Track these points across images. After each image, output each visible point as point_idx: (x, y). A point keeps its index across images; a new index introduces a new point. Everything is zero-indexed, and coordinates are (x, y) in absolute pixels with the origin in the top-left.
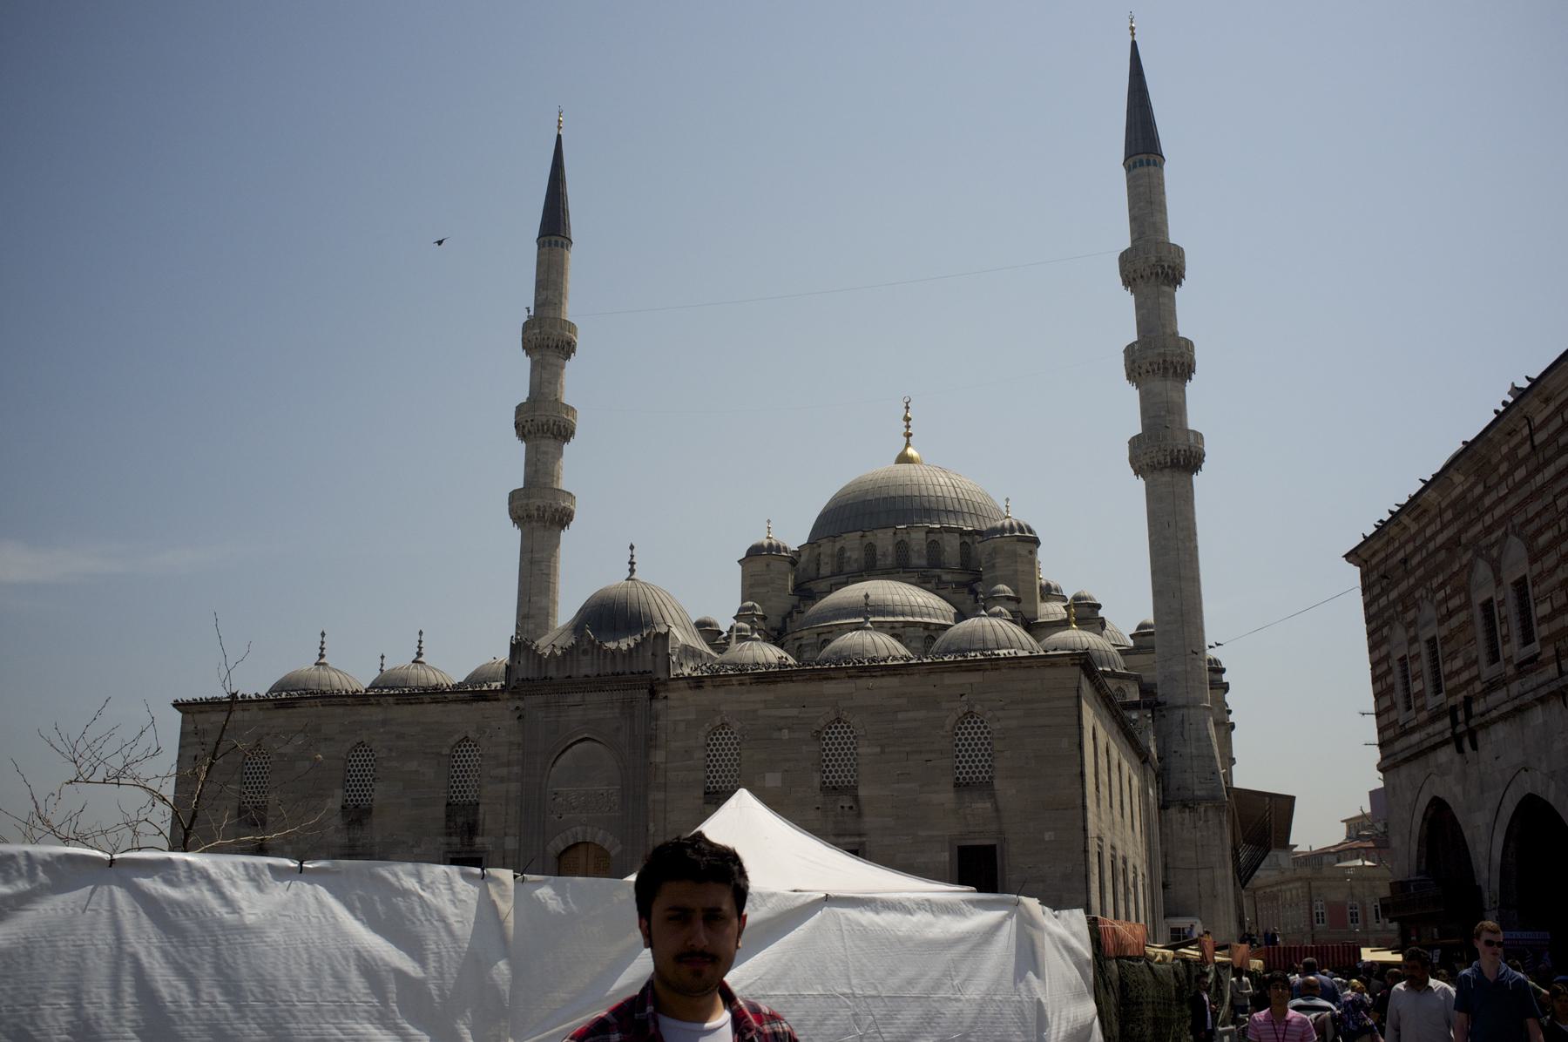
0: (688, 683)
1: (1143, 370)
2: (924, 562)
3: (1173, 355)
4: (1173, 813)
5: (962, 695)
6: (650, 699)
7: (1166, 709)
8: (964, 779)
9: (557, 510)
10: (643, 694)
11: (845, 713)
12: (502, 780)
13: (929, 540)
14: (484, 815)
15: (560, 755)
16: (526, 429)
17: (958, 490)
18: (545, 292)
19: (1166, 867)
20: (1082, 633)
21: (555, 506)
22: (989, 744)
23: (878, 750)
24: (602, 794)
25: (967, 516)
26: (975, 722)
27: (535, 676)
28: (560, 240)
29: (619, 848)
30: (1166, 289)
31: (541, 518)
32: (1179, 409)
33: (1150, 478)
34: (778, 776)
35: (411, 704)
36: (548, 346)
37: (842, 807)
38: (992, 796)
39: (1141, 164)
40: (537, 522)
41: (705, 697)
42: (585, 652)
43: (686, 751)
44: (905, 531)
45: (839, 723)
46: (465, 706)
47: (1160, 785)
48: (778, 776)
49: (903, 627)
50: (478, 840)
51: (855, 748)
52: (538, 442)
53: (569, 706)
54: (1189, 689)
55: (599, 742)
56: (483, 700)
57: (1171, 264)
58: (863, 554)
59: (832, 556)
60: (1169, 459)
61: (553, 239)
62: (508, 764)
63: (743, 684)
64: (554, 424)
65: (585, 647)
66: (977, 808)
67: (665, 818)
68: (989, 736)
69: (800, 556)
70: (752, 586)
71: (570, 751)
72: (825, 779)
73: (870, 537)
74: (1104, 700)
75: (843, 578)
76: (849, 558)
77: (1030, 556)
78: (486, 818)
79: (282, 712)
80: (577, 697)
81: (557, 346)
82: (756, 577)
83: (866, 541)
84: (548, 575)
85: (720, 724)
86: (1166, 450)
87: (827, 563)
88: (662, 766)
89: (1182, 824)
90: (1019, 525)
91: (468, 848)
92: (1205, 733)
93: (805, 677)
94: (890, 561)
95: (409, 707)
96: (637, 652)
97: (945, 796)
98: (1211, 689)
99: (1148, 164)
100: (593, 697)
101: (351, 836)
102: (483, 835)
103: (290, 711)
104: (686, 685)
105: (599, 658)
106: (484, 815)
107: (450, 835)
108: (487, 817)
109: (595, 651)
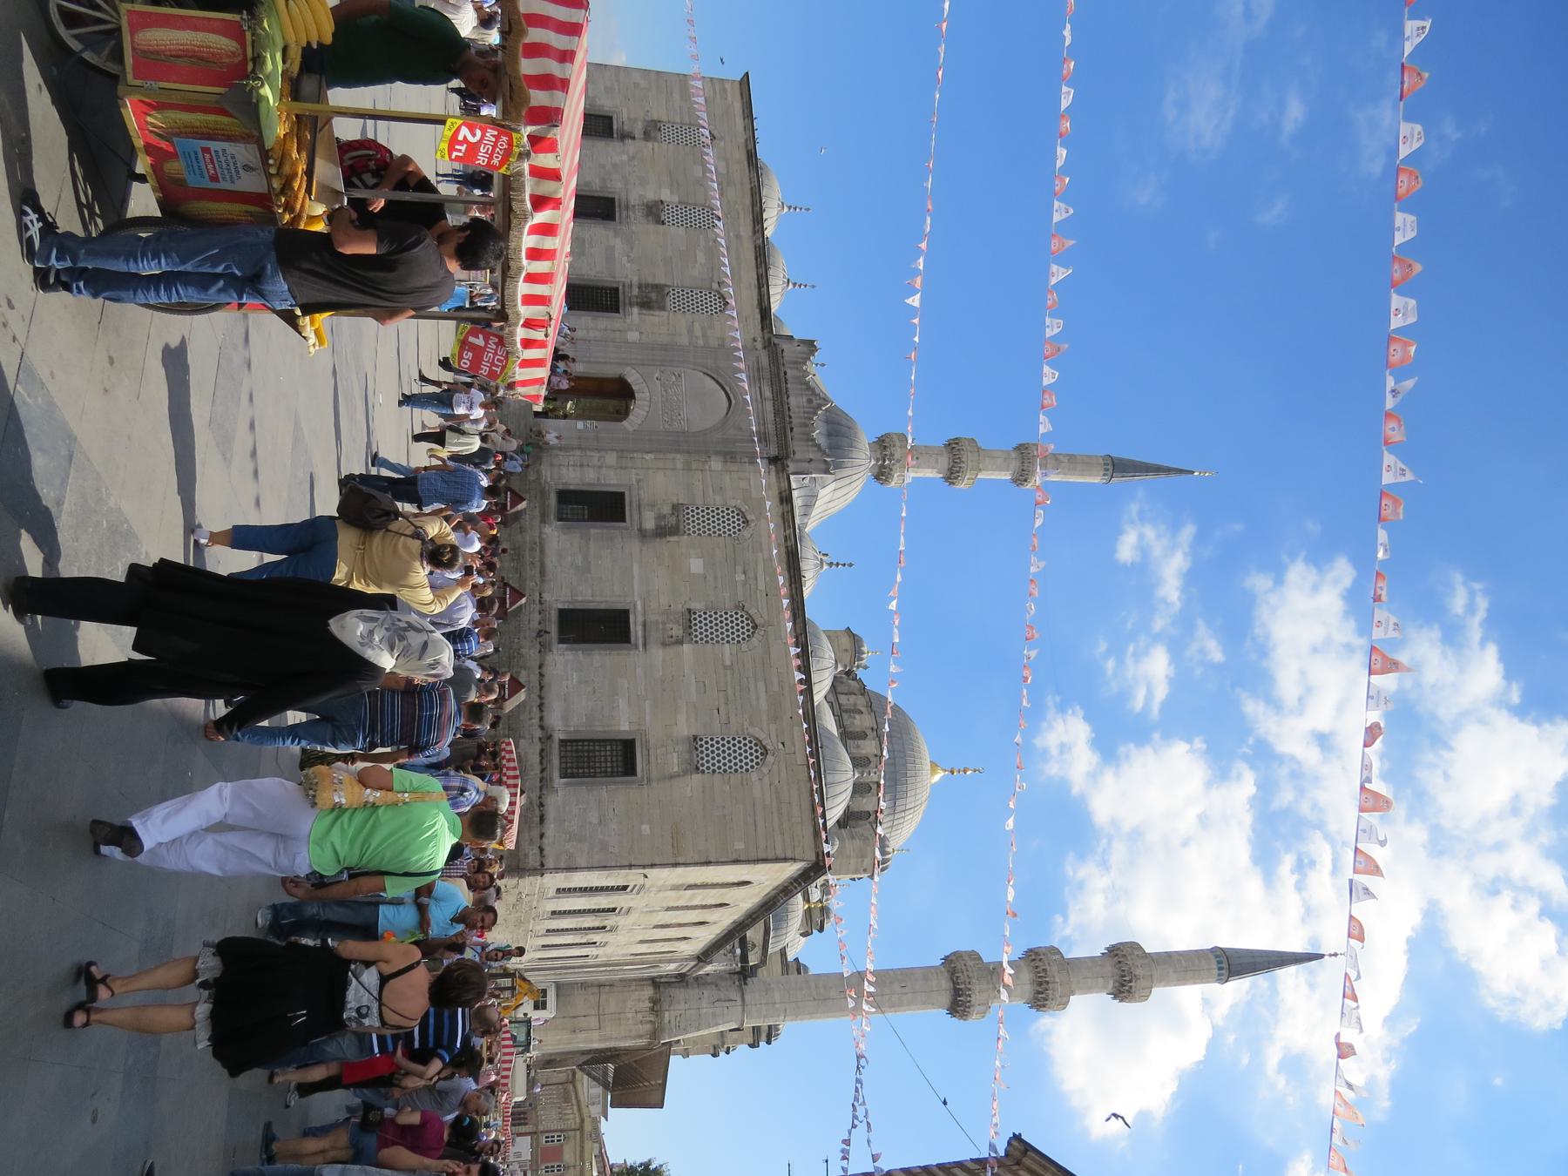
0: (785, 491)
1: (1038, 963)
3: (1054, 991)
4: (648, 992)
5: (783, 744)
6: (768, 458)
7: (741, 985)
8: (701, 746)
9: (891, 470)
10: (773, 451)
11: (762, 633)
12: (690, 331)
13: (872, 786)
14: (658, 316)
15: (713, 378)
17: (912, 811)
19: (600, 985)
20: (801, 912)
22: (736, 771)
23: (728, 663)
24: (680, 415)
25: (891, 817)
26: (757, 757)
27: (786, 359)
28: (1110, 473)
29: (630, 429)
33: (943, 969)
34: (701, 571)
35: (756, 259)
36: (1023, 463)
37: (672, 629)
38: (685, 772)
39: (1219, 962)
40: (881, 454)
42: (810, 401)
43: (721, 488)
45: (752, 627)
46: (756, 303)
47: (674, 980)
48: (701, 571)
50: (635, 310)
51: (728, 642)
53: (760, 388)
54: (758, 1006)
55: (727, 414)
56: (762, 317)
57: (1133, 989)
58: (857, 730)
59: (855, 705)
60: (962, 986)
61: (1110, 467)
62: (705, 336)
63: (786, 540)
64: (960, 467)
65: (815, 402)
66: (673, 757)
67: (658, 469)
68: (743, 770)
69: (853, 680)
71: (719, 388)
72: (698, 614)
74: (770, 900)
75: (837, 711)
76: (855, 718)
77: (862, 869)
78: (655, 318)
79: (744, 157)
80: (768, 394)
81: (1023, 470)
83: (869, 732)
85: (748, 518)
86: (969, 983)
87: (849, 700)
88: (707, 468)
89: (639, 1000)
90: (888, 860)
91: (627, 301)
92: (720, 1022)
93: (795, 596)
95: (753, 258)
96: (812, 446)
97: (684, 728)
98: (753, 1027)
99: (1220, 969)
100: (769, 406)
101: (637, 207)
102: (639, 314)
103: (746, 163)
104: (783, 489)
105: (804, 413)
106: (658, 316)
107: (640, 287)
108: (657, 318)
109: (811, 410)
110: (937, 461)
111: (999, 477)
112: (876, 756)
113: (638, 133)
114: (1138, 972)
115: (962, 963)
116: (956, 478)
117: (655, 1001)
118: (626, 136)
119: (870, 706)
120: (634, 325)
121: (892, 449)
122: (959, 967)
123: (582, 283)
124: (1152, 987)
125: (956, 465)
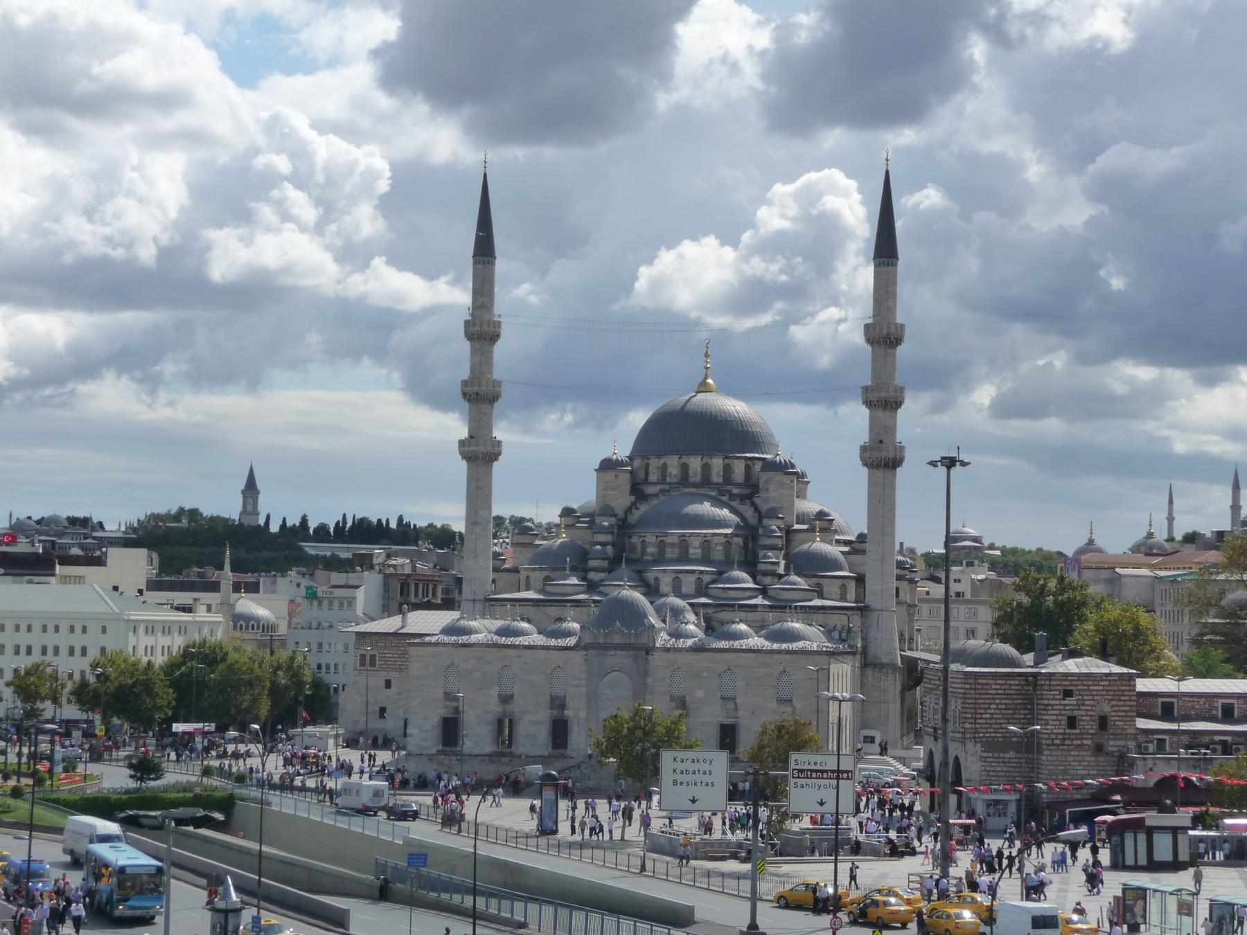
2: (721, 480)
12: (577, 686)
30: (891, 351)
31: (483, 459)
32: (892, 429)
38: (792, 705)
39: (884, 265)
41: (671, 656)
42: (617, 633)
50: (566, 712)
70: (604, 489)
73: (685, 459)
78: (570, 702)
80: (613, 652)
94: (698, 479)
97: (774, 705)
99: (888, 265)
100: (622, 653)
107: (552, 708)
113: (454, 704)
114: (885, 331)
117: (875, 666)
118: (456, 710)
120: (576, 712)
123: (551, 738)
124: (896, 324)
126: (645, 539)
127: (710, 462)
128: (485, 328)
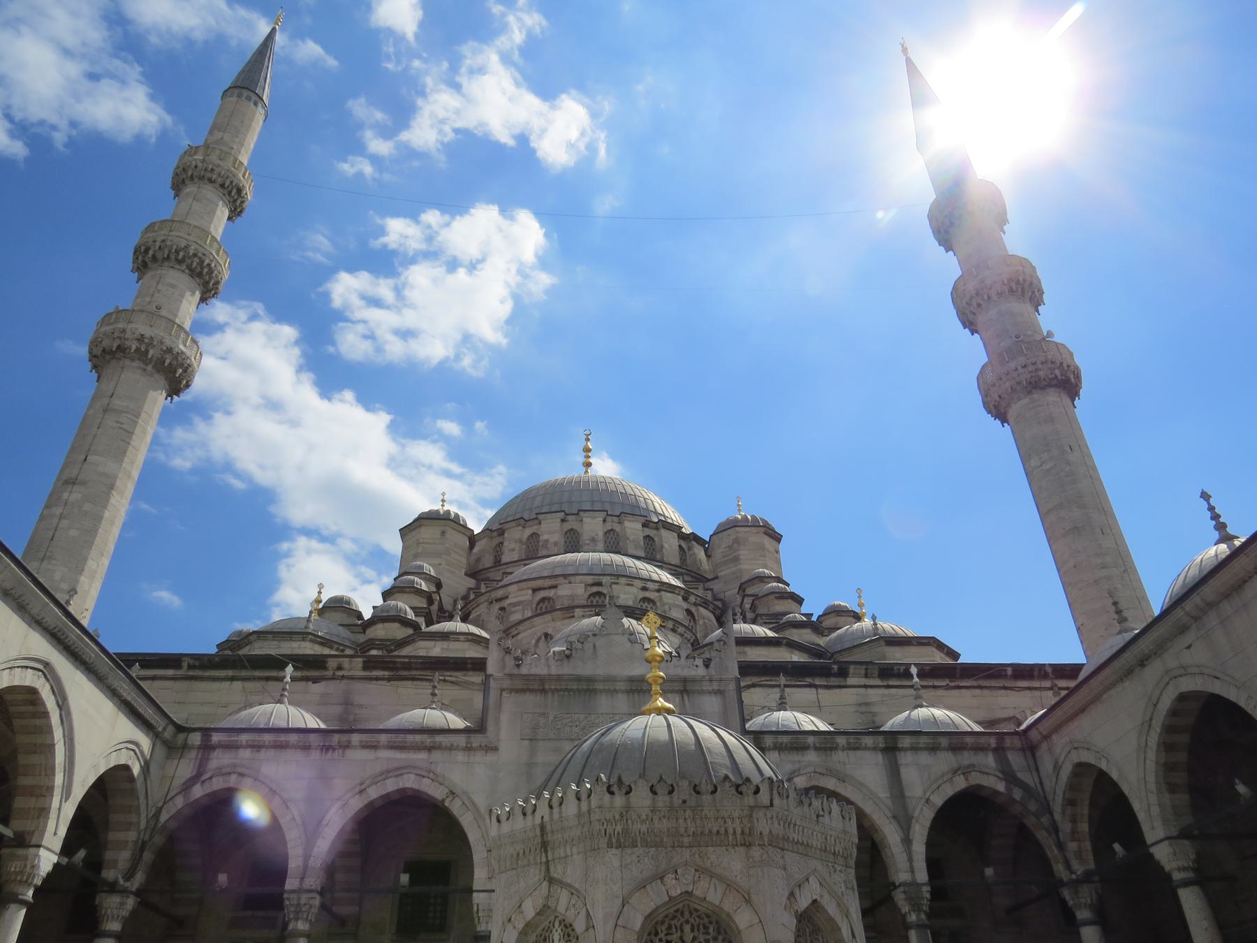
9: (170, 350)
16: (151, 253)
18: (221, 133)
21: (168, 343)
28: (254, 98)
31: (142, 355)
40: (132, 360)
44: (616, 519)
49: (658, 591)
52: (164, 272)
59: (520, 541)
61: (246, 93)
73: (572, 523)
76: (547, 541)
77: (775, 554)
82: (425, 545)
83: (567, 526)
84: (130, 433)
86: (1052, 363)
87: (513, 550)
110: (173, 286)
111: (255, 138)
112: (604, 521)
115: (1021, 370)
116: (211, 272)
119: (522, 522)
121: (128, 335)
122: (1028, 376)
125: (188, 261)
126: (505, 603)
127: (617, 528)
128: (214, 158)
